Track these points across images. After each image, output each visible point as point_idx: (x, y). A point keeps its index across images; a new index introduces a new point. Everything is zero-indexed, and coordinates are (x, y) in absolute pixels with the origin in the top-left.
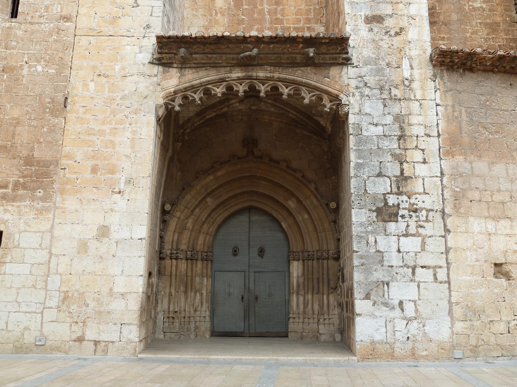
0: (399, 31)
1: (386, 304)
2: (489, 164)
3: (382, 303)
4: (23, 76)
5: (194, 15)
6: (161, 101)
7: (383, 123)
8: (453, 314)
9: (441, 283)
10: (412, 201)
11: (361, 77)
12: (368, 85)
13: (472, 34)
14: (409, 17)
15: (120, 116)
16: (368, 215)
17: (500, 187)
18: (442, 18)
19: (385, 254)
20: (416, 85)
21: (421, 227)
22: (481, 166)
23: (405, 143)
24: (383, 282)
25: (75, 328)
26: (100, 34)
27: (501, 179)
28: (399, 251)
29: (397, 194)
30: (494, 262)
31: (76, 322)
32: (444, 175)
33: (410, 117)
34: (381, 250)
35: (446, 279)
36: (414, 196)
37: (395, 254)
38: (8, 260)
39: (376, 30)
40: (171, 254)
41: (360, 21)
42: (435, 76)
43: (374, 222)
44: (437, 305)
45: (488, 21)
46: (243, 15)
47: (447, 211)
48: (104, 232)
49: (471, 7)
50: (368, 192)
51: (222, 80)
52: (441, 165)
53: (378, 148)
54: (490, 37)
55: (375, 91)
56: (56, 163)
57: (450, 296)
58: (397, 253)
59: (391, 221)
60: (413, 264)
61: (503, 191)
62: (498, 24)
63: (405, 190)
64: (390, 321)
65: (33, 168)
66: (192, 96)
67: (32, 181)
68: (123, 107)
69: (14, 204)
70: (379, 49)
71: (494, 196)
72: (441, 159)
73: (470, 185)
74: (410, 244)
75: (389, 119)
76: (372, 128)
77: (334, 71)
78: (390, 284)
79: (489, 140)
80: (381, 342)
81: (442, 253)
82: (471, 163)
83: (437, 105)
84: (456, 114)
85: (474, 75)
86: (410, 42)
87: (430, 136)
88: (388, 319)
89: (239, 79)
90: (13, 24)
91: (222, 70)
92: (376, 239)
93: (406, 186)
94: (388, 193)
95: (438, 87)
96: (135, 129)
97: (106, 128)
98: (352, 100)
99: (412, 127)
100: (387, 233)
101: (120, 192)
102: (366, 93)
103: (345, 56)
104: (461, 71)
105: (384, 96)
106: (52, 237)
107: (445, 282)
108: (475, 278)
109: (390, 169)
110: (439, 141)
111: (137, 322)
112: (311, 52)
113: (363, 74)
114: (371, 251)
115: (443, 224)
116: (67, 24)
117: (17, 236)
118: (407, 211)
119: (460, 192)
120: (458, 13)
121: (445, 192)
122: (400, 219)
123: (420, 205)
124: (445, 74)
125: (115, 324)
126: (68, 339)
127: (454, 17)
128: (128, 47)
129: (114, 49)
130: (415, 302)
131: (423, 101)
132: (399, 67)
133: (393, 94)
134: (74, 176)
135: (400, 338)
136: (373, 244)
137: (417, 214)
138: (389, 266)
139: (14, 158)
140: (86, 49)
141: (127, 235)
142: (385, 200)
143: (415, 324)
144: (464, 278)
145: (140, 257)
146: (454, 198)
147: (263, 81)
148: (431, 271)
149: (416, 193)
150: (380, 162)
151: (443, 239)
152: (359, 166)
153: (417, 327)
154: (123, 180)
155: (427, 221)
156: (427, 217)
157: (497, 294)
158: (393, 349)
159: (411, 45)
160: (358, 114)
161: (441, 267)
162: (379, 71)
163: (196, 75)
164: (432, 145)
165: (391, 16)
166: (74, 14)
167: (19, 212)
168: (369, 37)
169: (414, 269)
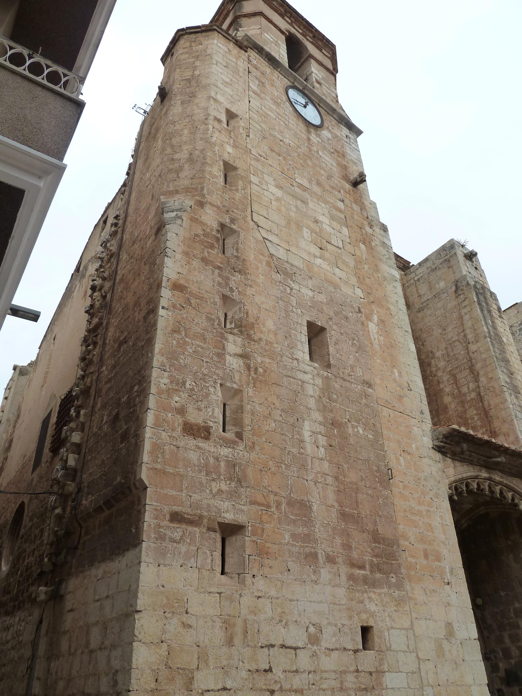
4: (350, 435)
15: (428, 498)
51: (476, 477)
66: (461, 488)
69: (375, 590)
96: (441, 514)
97: (422, 508)
101: (448, 584)
117: (386, 634)
129: (407, 426)
134: (413, 561)
139: (364, 532)
140: (389, 421)
154: (447, 570)
167: (382, 601)
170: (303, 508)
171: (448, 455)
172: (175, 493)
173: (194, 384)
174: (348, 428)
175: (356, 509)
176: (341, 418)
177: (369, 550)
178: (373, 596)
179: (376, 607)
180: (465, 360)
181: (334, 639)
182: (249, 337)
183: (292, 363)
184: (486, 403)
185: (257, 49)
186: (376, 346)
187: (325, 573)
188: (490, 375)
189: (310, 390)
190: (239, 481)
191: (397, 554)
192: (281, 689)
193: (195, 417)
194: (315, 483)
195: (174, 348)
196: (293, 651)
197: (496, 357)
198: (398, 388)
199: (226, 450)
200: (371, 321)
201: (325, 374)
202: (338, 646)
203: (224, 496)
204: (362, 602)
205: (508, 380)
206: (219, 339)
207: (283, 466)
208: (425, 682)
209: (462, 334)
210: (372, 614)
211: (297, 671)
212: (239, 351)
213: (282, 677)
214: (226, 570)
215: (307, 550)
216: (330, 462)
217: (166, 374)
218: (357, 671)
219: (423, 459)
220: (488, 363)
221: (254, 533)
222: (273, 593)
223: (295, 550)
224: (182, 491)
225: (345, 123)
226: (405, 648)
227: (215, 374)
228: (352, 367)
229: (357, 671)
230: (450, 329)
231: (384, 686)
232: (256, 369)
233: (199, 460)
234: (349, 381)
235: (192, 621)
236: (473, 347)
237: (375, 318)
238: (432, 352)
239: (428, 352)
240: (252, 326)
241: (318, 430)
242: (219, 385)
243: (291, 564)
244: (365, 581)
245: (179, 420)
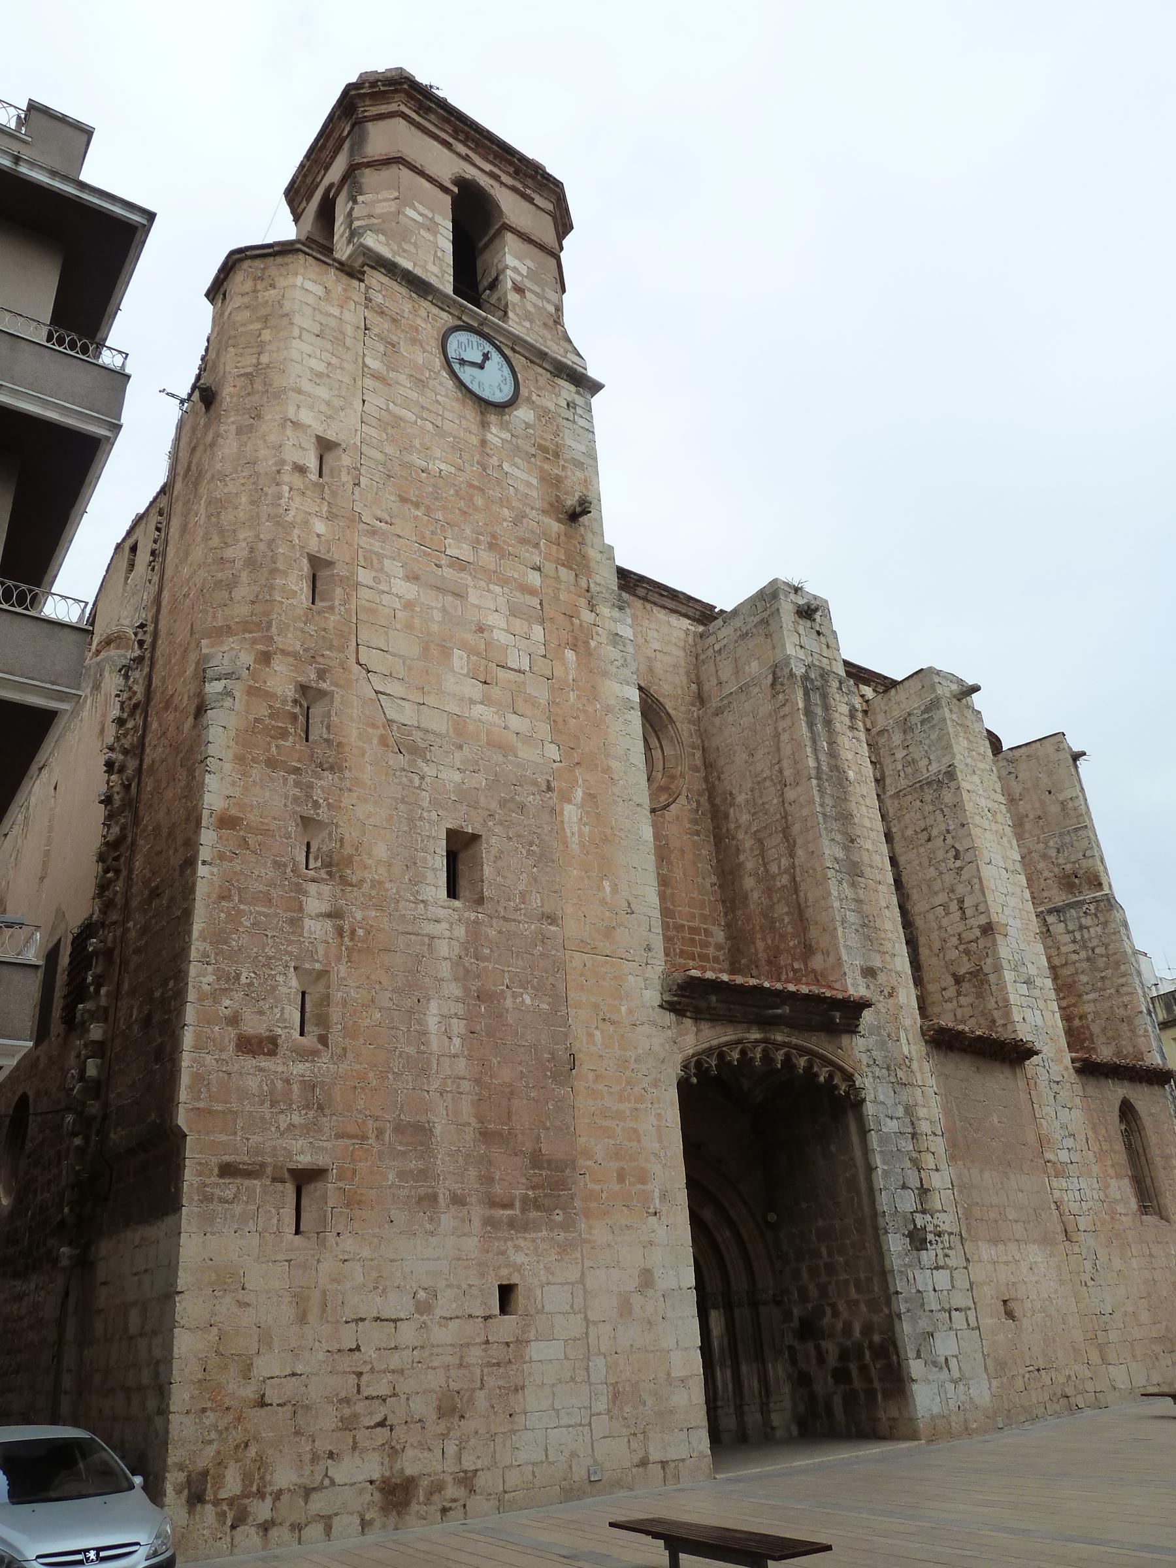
1: (935, 1364)
4: (507, 1010)
10: (935, 1221)
15: (637, 1090)
20: (915, 1066)
31: (635, 1434)
38: (532, 1336)
51: (739, 1042)
56: (572, 1163)
60: (947, 1307)
66: (708, 1063)
67: (546, 1196)
68: (640, 1075)
69: (527, 1235)
74: (942, 1278)
75: (900, 1112)
77: (845, 1040)
97: (626, 1107)
106: (585, 1290)
116: (553, 928)
117: (538, 1292)
123: (943, 1227)
125: (681, 1430)
126: (629, 1464)
129: (615, 977)
130: (956, 1357)
134: (597, 1187)
139: (516, 1155)
140: (582, 975)
141: (674, 1285)
142: (914, 1220)
154: (657, 1194)
158: (949, 1423)
167: (536, 1249)
170: (418, 1134)
171: (688, 1014)
172: (225, 1138)
173: (253, 975)
174: (505, 999)
175: (506, 1124)
176: (495, 985)
177: (524, 1180)
178: (521, 1243)
179: (525, 1259)
180: (778, 816)
181: (454, 1305)
182: (344, 881)
183: (416, 909)
184: (802, 894)
185: (384, 267)
186: (575, 847)
187: (447, 1220)
188: (811, 847)
189: (443, 949)
190: (321, 1108)
191: (570, 1180)
192: (372, 1370)
193: (254, 1026)
194: (441, 1094)
195: (222, 925)
196: (392, 1324)
197: (824, 815)
198: (608, 914)
199: (301, 1066)
200: (569, 801)
201: (473, 916)
202: (460, 1314)
203: (297, 1132)
204: (503, 1253)
205: (841, 854)
206: (293, 894)
207: (390, 1076)
208: (593, 1350)
209: (777, 767)
210: (518, 1269)
211: (396, 1348)
212: (325, 907)
213: (374, 1356)
214: (302, 1229)
215: (422, 1191)
216: (469, 1058)
217: (210, 969)
218: (487, 1342)
220: (809, 825)
221: (340, 1178)
222: (366, 1253)
223: (403, 1193)
224: (236, 1133)
225: (568, 375)
226: (568, 1308)
227: (287, 952)
228: (523, 895)
229: (487, 1342)
230: (759, 754)
231: (527, 1358)
232: (353, 932)
233: (260, 1087)
234: (514, 920)
235: (250, 1298)
236: (790, 794)
237: (579, 793)
238: (731, 794)
239: (725, 793)
240: (349, 861)
241: (453, 1011)
242: (292, 969)
243: (394, 1213)
244: (512, 1224)
245: (232, 1033)
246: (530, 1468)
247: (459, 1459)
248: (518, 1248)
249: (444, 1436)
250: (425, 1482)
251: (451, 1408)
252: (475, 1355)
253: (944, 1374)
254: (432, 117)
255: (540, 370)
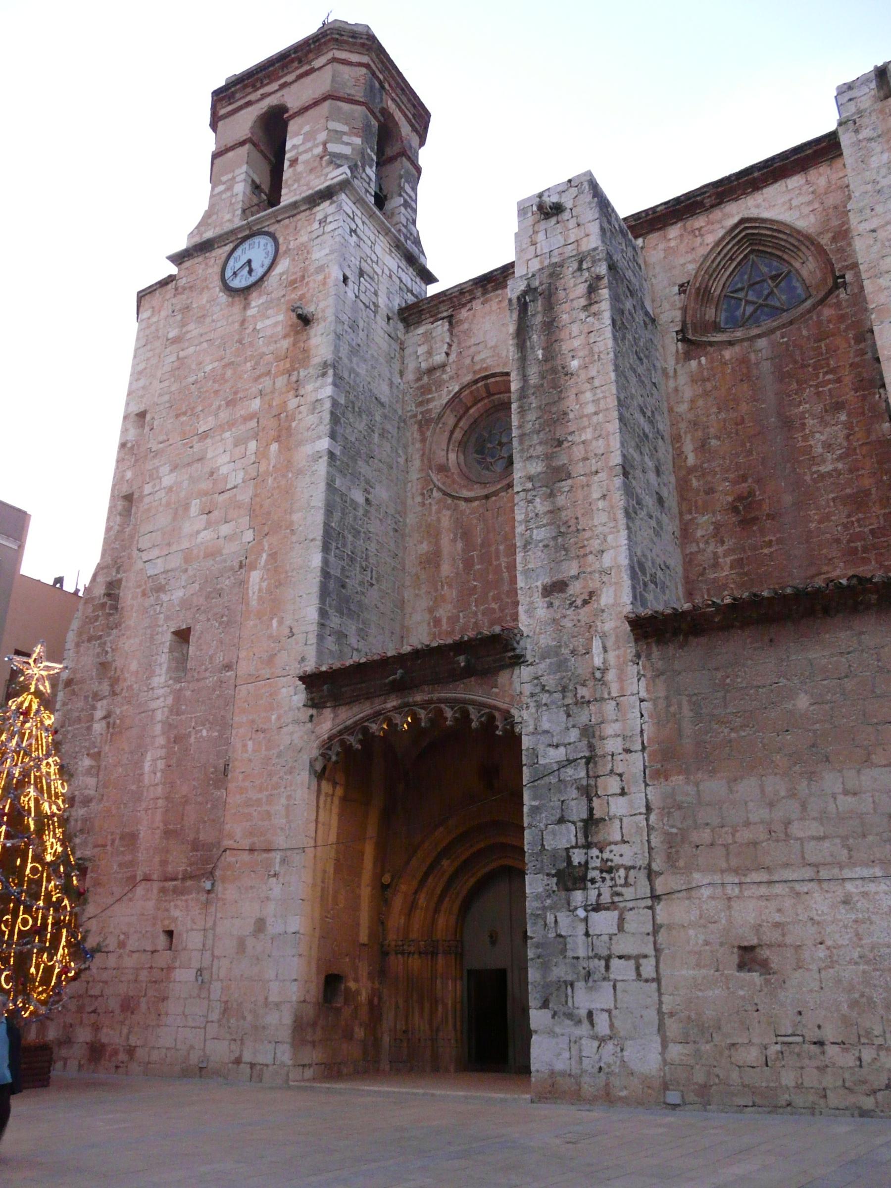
0: (587, 598)
1: (570, 1016)
2: (728, 783)
3: (564, 1014)
5: (417, 595)
6: (315, 753)
7: (566, 742)
8: (665, 1032)
9: (647, 981)
10: (606, 855)
11: (537, 678)
12: (547, 688)
13: (820, 522)
14: (600, 573)
15: (275, 779)
16: (545, 882)
17: (748, 818)
18: (766, 507)
19: (568, 939)
20: (611, 676)
21: (619, 894)
22: (714, 786)
23: (596, 767)
24: (565, 982)
25: (233, 1047)
26: (258, 678)
27: (751, 805)
28: (587, 934)
29: (584, 847)
30: (736, 944)
31: (235, 1040)
32: (651, 809)
33: (602, 725)
34: (563, 933)
35: (654, 975)
36: (608, 848)
37: (581, 939)
38: (177, 964)
39: (557, 603)
40: (396, 946)
41: (536, 595)
42: (638, 656)
43: (554, 891)
44: (641, 1016)
45: (848, 491)
46: (474, 580)
47: (655, 867)
48: (260, 925)
49: (815, 476)
50: (546, 847)
51: (377, 714)
52: (646, 795)
53: (560, 780)
54: (854, 519)
55: (555, 695)
57: (661, 1003)
58: (584, 937)
59: (576, 889)
60: (605, 953)
61: (755, 824)
62: (867, 493)
63: (595, 840)
64: (575, 1042)
65: (199, 854)
69: (183, 898)
70: (561, 631)
71: (738, 835)
72: (646, 785)
73: (695, 821)
74: (603, 922)
76: (552, 752)
77: (503, 677)
78: (576, 984)
79: (730, 741)
80: (563, 1074)
81: (648, 934)
82: (697, 784)
83: (642, 701)
84: (672, 709)
85: (703, 640)
86: (603, 611)
87: (631, 752)
88: (573, 1039)
89: (395, 708)
90: (183, 684)
91: (377, 700)
92: (556, 917)
93: (597, 833)
94: (572, 847)
95: (642, 672)
97: (263, 796)
98: (525, 714)
99: (605, 742)
100: (571, 908)
101: (275, 875)
102: (544, 702)
103: (511, 654)
104: (681, 638)
105: (569, 700)
106: (214, 935)
107: (653, 980)
108: (704, 971)
109: (574, 810)
110: (644, 757)
111: (289, 1040)
112: (462, 660)
113: (540, 673)
114: (550, 936)
115: (649, 887)
116: (228, 674)
117: (185, 935)
118: (598, 872)
119: (676, 834)
120: (794, 490)
121: (652, 837)
122: (589, 884)
123: (617, 860)
124: (654, 649)
125: (270, 1042)
126: (227, 1061)
127: (788, 499)
128: (284, 690)
130: (609, 1011)
131: (622, 698)
132: (588, 653)
133: (579, 696)
135: (589, 1068)
136: (553, 925)
137: (612, 875)
138: (574, 958)
143: (610, 1047)
144: (684, 972)
145: (293, 956)
146: (668, 845)
147: (424, 705)
148: (632, 963)
149: (610, 843)
150: (563, 801)
151: (650, 912)
152: (535, 810)
153: (612, 1052)
155: (626, 884)
156: (626, 878)
157: (743, 998)
158: (579, 1084)
159: (605, 615)
160: (533, 733)
161: (646, 956)
162: (561, 665)
163: (350, 714)
164: (636, 763)
165: (577, 577)
166: (234, 661)
167: (187, 907)
168: (549, 616)
169: (608, 959)
170: (130, 839)
177: (185, 860)
181: (137, 944)
185: (184, 257)
186: (254, 603)
189: (159, 716)
204: (167, 910)
208: (215, 977)
210: (175, 920)
211: (106, 968)
219: (285, 730)
223: (120, 876)
225: (320, 198)
229: (151, 968)
246: (164, 1051)
247: (128, 1039)
248: (176, 906)
249: (122, 1023)
250: (109, 1049)
251: (128, 1006)
252: (144, 975)
253: (584, 1029)
254: (238, 96)
255: (303, 215)
